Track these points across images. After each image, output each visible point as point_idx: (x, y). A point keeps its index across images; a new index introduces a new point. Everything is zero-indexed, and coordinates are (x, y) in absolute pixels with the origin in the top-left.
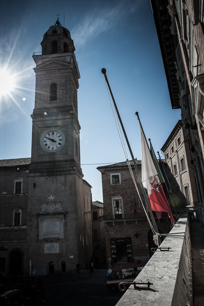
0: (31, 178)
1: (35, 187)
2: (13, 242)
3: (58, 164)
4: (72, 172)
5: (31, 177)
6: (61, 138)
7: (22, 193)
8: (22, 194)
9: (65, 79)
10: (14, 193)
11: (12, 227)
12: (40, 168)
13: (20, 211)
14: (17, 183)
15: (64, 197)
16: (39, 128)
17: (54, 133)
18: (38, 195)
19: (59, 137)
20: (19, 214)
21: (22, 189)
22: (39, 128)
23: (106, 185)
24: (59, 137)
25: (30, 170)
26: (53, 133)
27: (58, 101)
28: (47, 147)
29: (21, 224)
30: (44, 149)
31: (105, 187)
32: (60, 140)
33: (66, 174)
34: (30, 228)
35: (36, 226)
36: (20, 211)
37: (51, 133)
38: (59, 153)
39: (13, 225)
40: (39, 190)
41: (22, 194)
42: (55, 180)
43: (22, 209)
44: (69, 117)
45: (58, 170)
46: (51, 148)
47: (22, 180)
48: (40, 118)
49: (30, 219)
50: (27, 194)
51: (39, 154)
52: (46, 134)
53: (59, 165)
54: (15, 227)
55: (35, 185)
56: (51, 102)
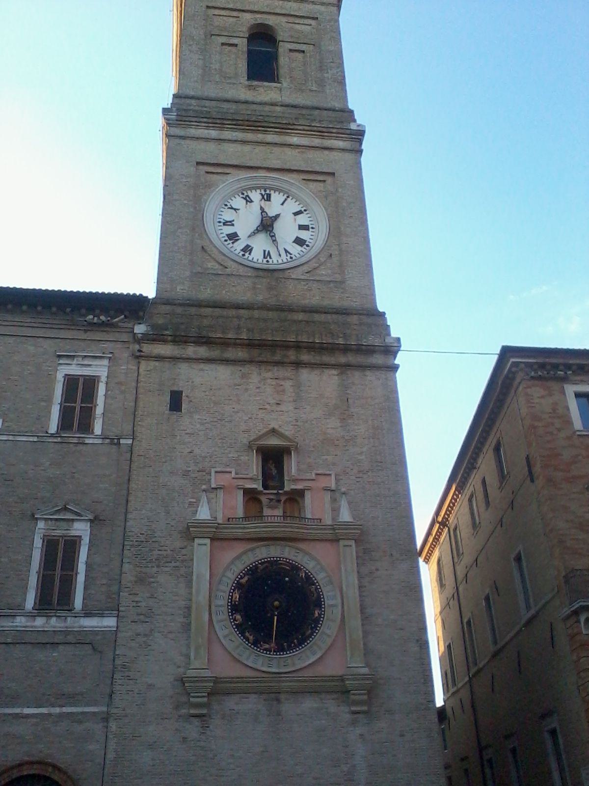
0: (157, 364)
1: (181, 411)
2: (17, 716)
3: (301, 316)
4: (378, 359)
5: (159, 358)
6: (303, 220)
7: (98, 429)
8: (100, 441)
9: (313, 22)
10: (53, 428)
11: (20, 622)
12: (206, 322)
13: (81, 529)
14: (71, 382)
15: (345, 473)
16: (198, 163)
17: (269, 196)
18: (197, 451)
19: (296, 214)
20: (73, 544)
21: (99, 410)
22: (201, 167)
23: (551, 433)
24: (296, 214)
25: (153, 326)
26: (268, 198)
27: (285, 85)
28: (239, 246)
29: (78, 602)
30: (225, 251)
31: (549, 442)
32: (302, 227)
33: (348, 366)
34: (140, 628)
35: (182, 620)
36: (81, 529)
37: (255, 196)
38: (303, 277)
39: (30, 602)
40: (202, 424)
41: (97, 437)
42: (288, 384)
43: (95, 521)
44: (340, 144)
45: (304, 338)
46: (257, 255)
47: (100, 369)
48: (208, 128)
49: (141, 580)
50: (130, 442)
51: (199, 269)
52: (233, 195)
53: (307, 322)
54: (40, 622)
55: (176, 402)
56: (255, 83)
